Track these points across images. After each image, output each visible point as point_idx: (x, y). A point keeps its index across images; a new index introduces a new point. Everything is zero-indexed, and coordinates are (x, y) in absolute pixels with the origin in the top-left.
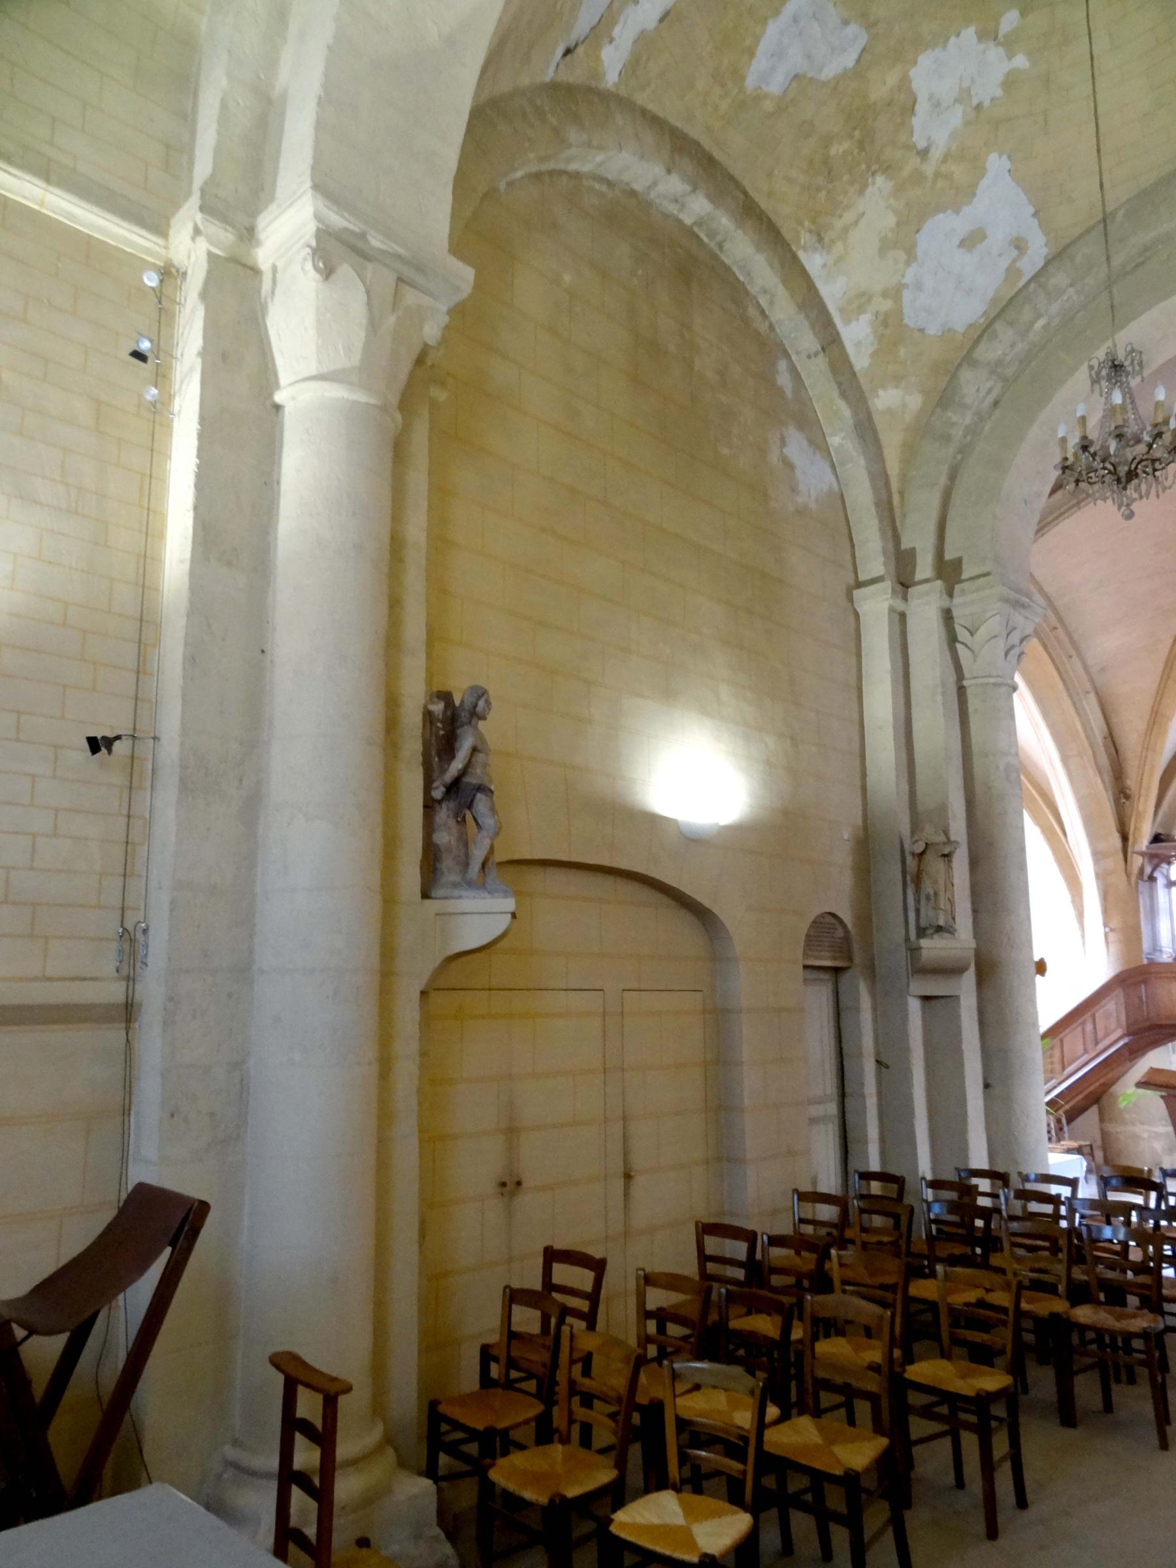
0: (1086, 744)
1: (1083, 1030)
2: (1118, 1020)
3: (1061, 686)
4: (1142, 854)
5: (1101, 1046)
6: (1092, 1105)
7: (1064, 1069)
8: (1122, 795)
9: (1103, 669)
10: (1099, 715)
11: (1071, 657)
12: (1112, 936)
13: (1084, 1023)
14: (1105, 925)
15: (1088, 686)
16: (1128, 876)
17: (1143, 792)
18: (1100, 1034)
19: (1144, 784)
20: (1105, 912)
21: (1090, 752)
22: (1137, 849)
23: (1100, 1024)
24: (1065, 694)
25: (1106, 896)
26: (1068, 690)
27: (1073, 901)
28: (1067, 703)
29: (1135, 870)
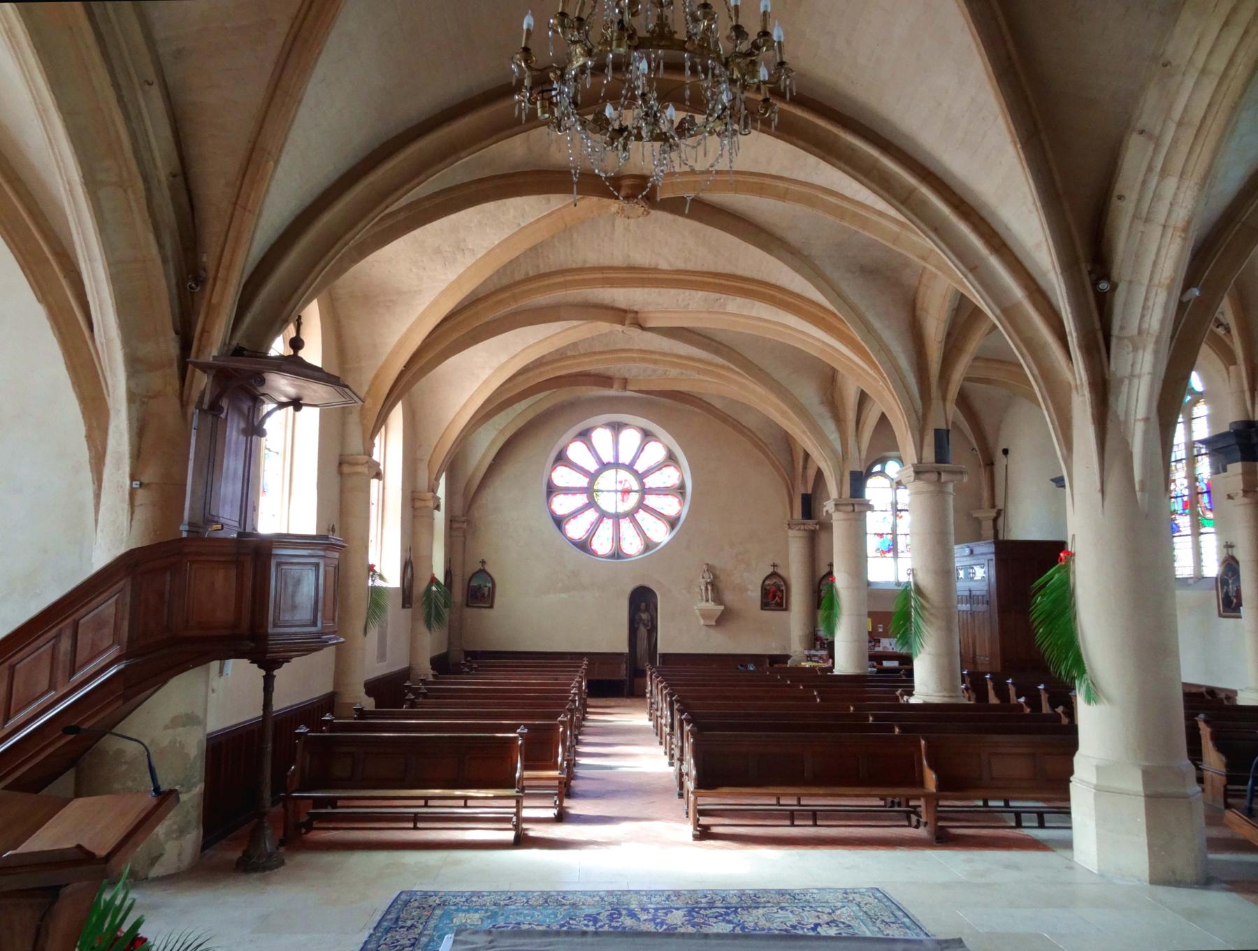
0: (134, 168)
1: (54, 648)
2: (116, 627)
3: (90, 38)
4: (205, 368)
5: (78, 677)
9: (179, 54)
10: (166, 132)
12: (141, 495)
13: (58, 637)
14: (133, 478)
15: (151, 74)
16: (184, 404)
18: (82, 654)
19: (225, 261)
20: (138, 455)
21: (140, 185)
22: (202, 359)
23: (84, 639)
24: (96, 55)
25: (140, 431)
27: (89, 437)
29: (195, 396)
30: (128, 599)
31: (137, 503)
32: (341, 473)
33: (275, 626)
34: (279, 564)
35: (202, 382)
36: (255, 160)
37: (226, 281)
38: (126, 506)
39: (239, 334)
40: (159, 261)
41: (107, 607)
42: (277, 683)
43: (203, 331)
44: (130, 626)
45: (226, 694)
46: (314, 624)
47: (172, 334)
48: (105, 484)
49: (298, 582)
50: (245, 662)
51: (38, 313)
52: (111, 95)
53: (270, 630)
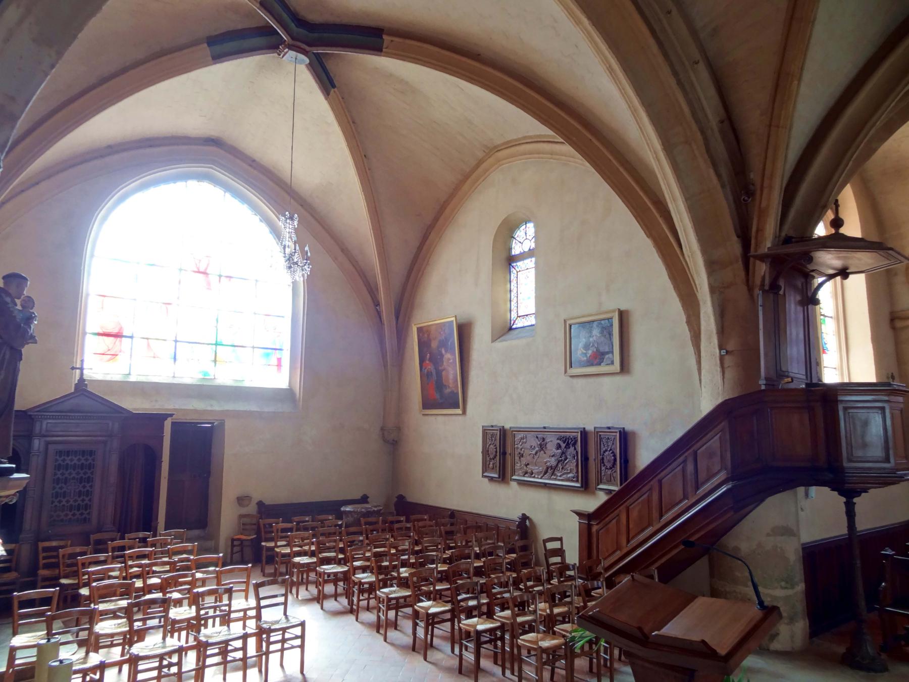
0: (694, 127)
1: (684, 471)
2: (722, 458)
3: (654, 48)
4: (762, 258)
6: (703, 555)
7: (661, 516)
8: (743, 192)
10: (712, 91)
11: (669, 12)
12: (728, 360)
13: (685, 461)
14: (721, 348)
15: (697, 56)
16: (750, 289)
17: (766, 182)
18: (702, 476)
19: (767, 173)
20: (722, 332)
23: (702, 464)
24: (660, 59)
25: (721, 313)
26: (666, 56)
28: (665, 72)
29: (758, 281)
30: (728, 437)
31: (726, 365)
32: (893, 328)
33: (850, 461)
34: (845, 409)
35: (762, 269)
36: (782, 82)
37: (771, 187)
38: (719, 369)
39: (786, 227)
40: (719, 187)
41: (714, 441)
42: (858, 509)
43: (757, 231)
44: (732, 456)
45: (815, 514)
46: (887, 460)
47: (735, 238)
48: (703, 354)
49: (866, 423)
50: (826, 489)
51: (648, 243)
52: (673, 82)
53: (846, 464)
